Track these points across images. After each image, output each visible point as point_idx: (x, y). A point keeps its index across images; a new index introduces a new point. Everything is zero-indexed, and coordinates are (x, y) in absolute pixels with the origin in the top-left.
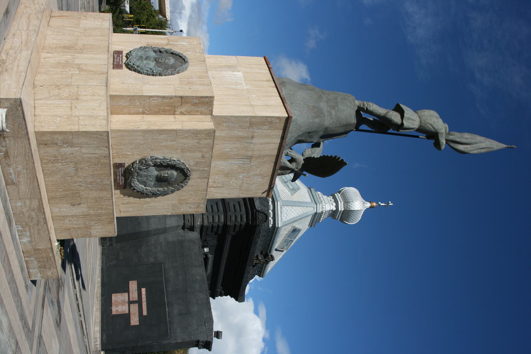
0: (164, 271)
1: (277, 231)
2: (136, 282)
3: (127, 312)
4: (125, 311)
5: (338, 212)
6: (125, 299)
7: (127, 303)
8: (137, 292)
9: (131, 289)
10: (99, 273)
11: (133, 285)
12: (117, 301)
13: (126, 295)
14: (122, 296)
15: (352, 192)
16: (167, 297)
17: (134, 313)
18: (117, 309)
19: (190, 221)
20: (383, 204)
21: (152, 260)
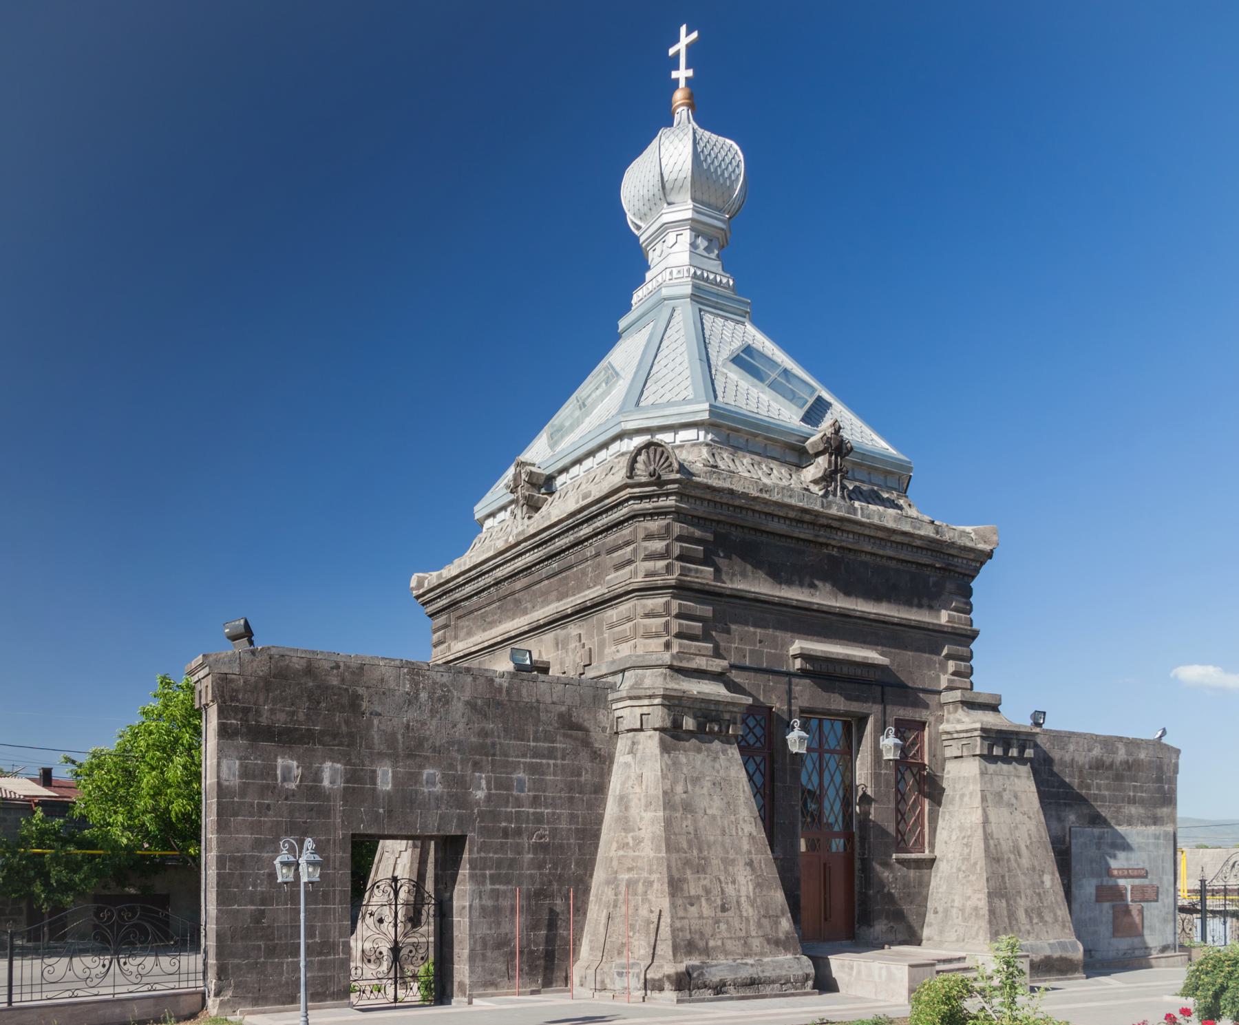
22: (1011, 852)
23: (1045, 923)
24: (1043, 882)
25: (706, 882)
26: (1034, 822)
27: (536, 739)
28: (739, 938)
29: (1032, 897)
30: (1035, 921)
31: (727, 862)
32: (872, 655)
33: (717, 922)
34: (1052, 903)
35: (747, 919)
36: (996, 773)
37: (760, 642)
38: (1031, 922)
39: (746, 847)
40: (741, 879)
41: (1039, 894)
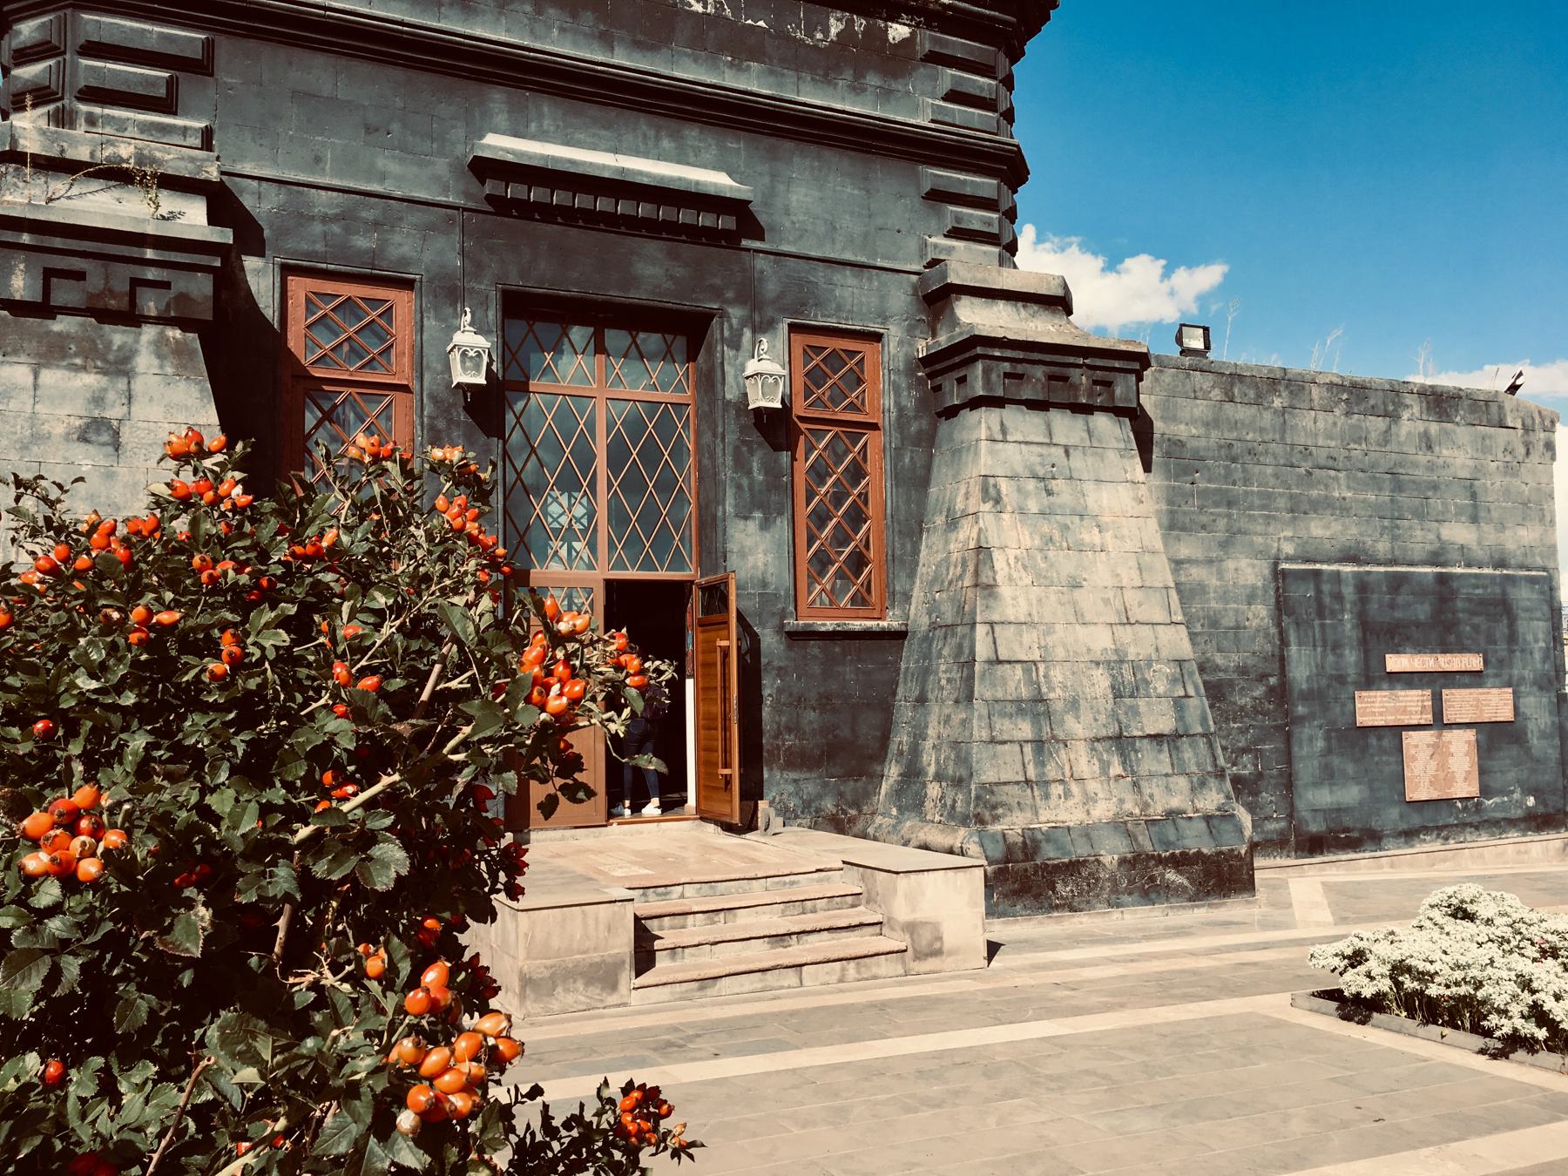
0: (1307, 561)
2: (1364, 694)
3: (1470, 735)
4: (1468, 742)
6: (1428, 746)
7: (1440, 736)
8: (1402, 693)
9: (1391, 720)
10: (1411, 865)
11: (1374, 708)
12: (1434, 776)
13: (1411, 739)
14: (1414, 759)
16: (1411, 564)
17: (1477, 706)
18: (1460, 776)
21: (1260, 614)
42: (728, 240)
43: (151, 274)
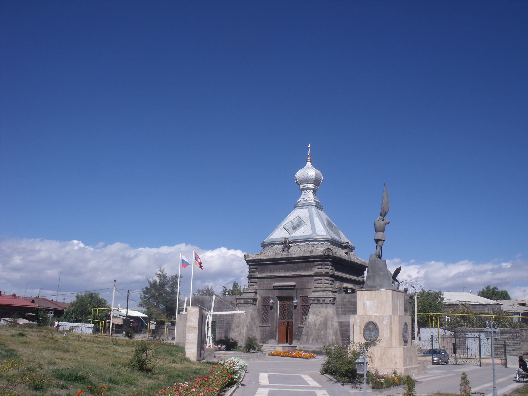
1: (333, 240)
5: (315, 189)
15: (300, 174)
19: (330, 300)
20: (309, 152)
22: (313, 325)
23: (318, 342)
24: (321, 333)
25: (238, 329)
26: (323, 318)
27: (227, 306)
28: (241, 339)
29: (316, 336)
30: (314, 341)
31: (243, 326)
32: (293, 283)
33: (238, 336)
34: (322, 338)
35: (244, 336)
36: (315, 307)
37: (267, 284)
38: (313, 341)
39: (247, 323)
40: (245, 329)
41: (318, 336)
42: (294, 289)
43: (249, 300)
